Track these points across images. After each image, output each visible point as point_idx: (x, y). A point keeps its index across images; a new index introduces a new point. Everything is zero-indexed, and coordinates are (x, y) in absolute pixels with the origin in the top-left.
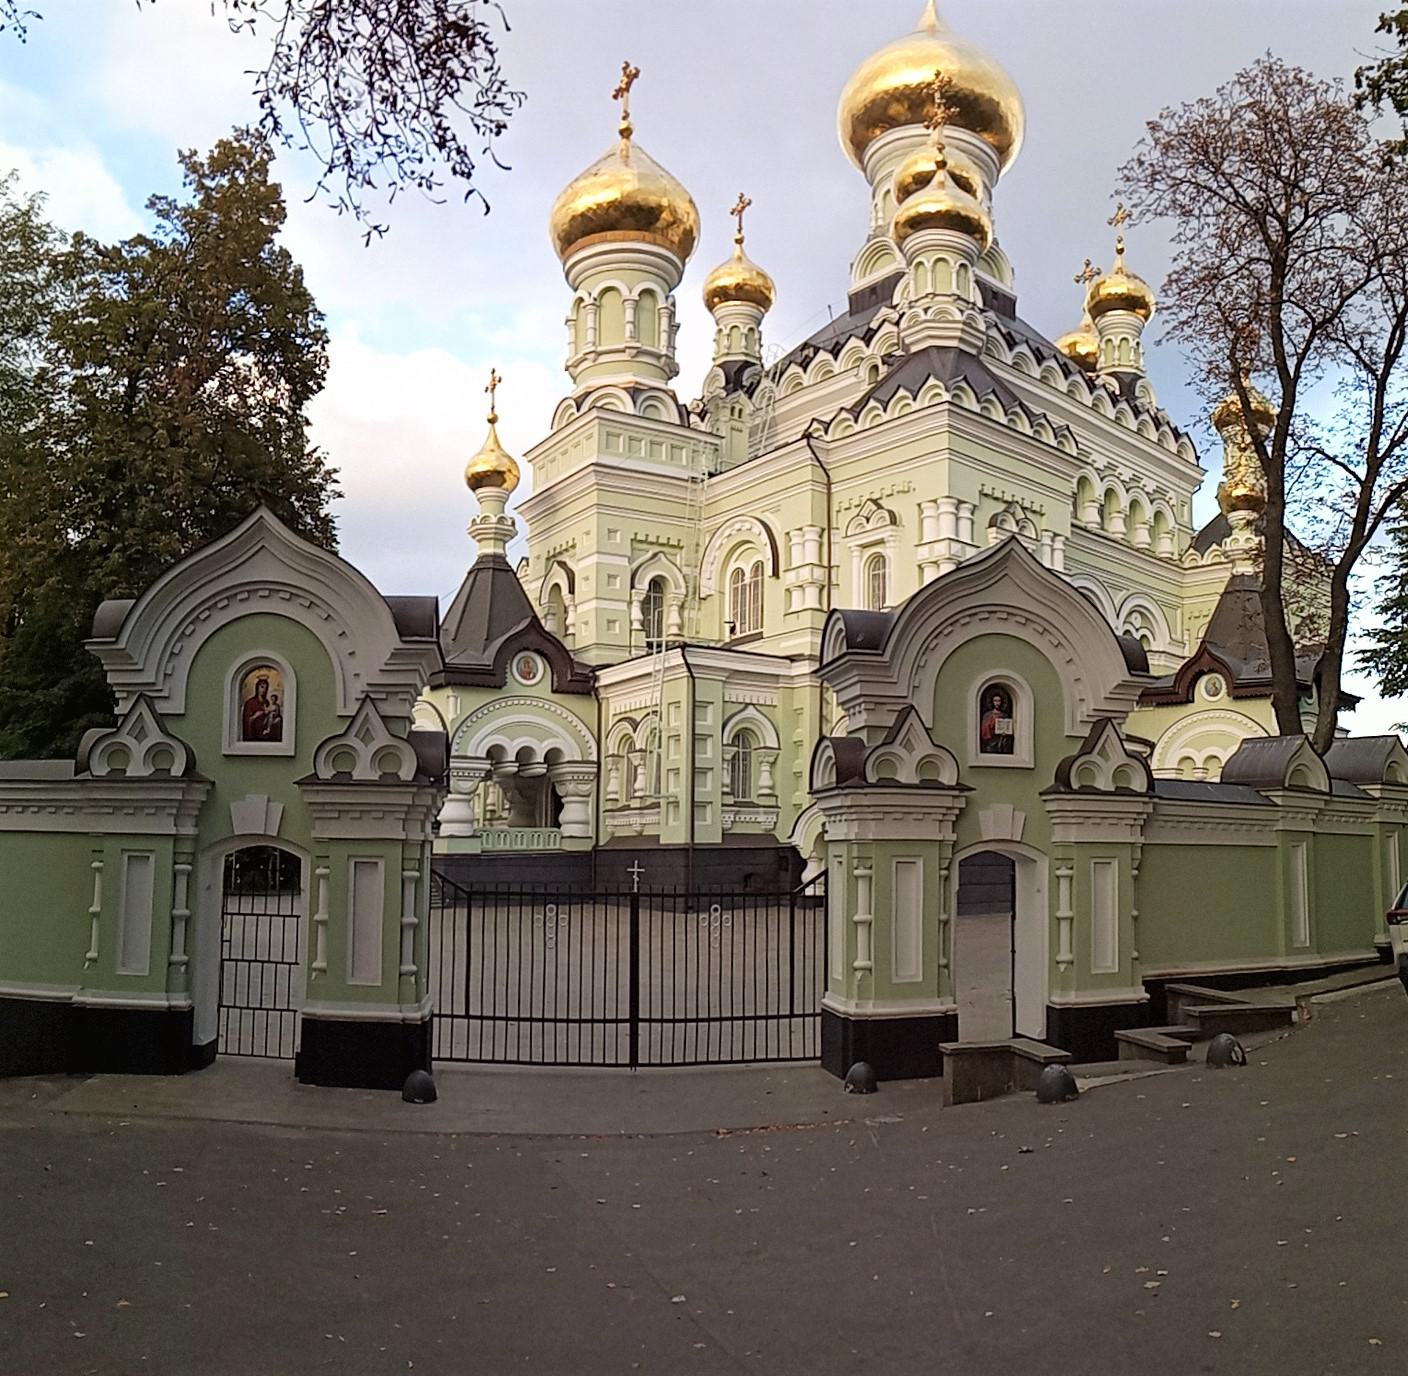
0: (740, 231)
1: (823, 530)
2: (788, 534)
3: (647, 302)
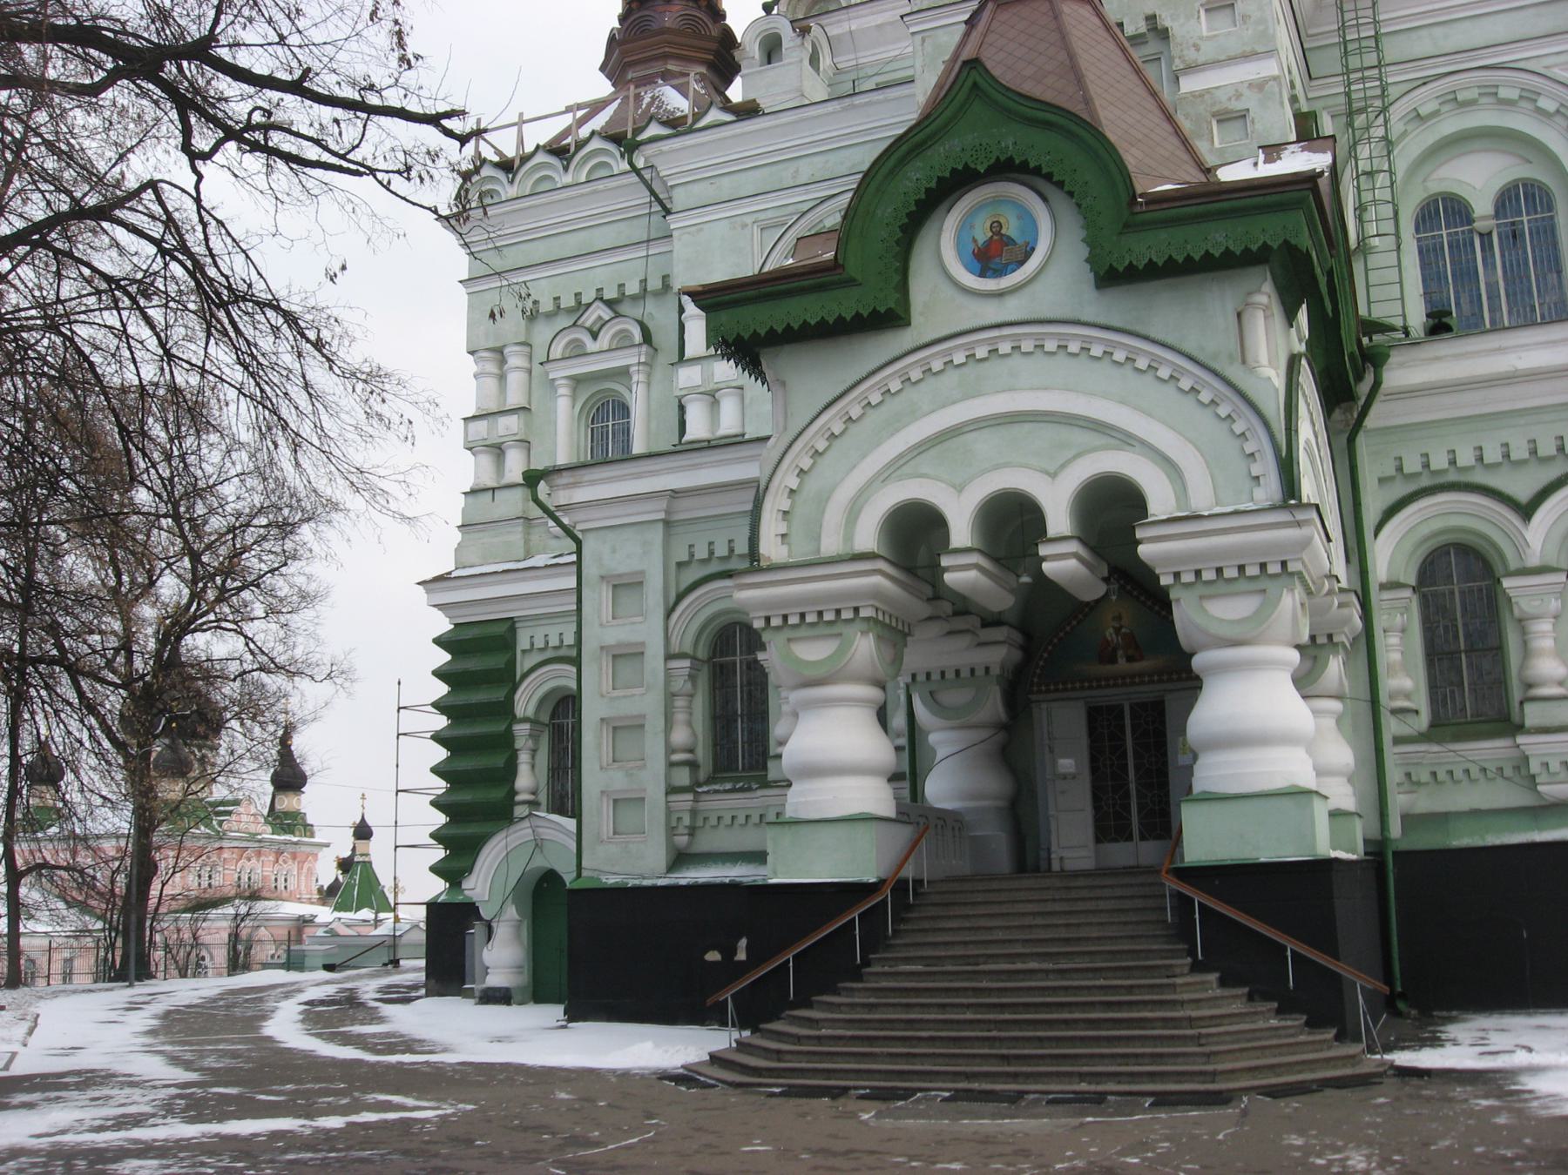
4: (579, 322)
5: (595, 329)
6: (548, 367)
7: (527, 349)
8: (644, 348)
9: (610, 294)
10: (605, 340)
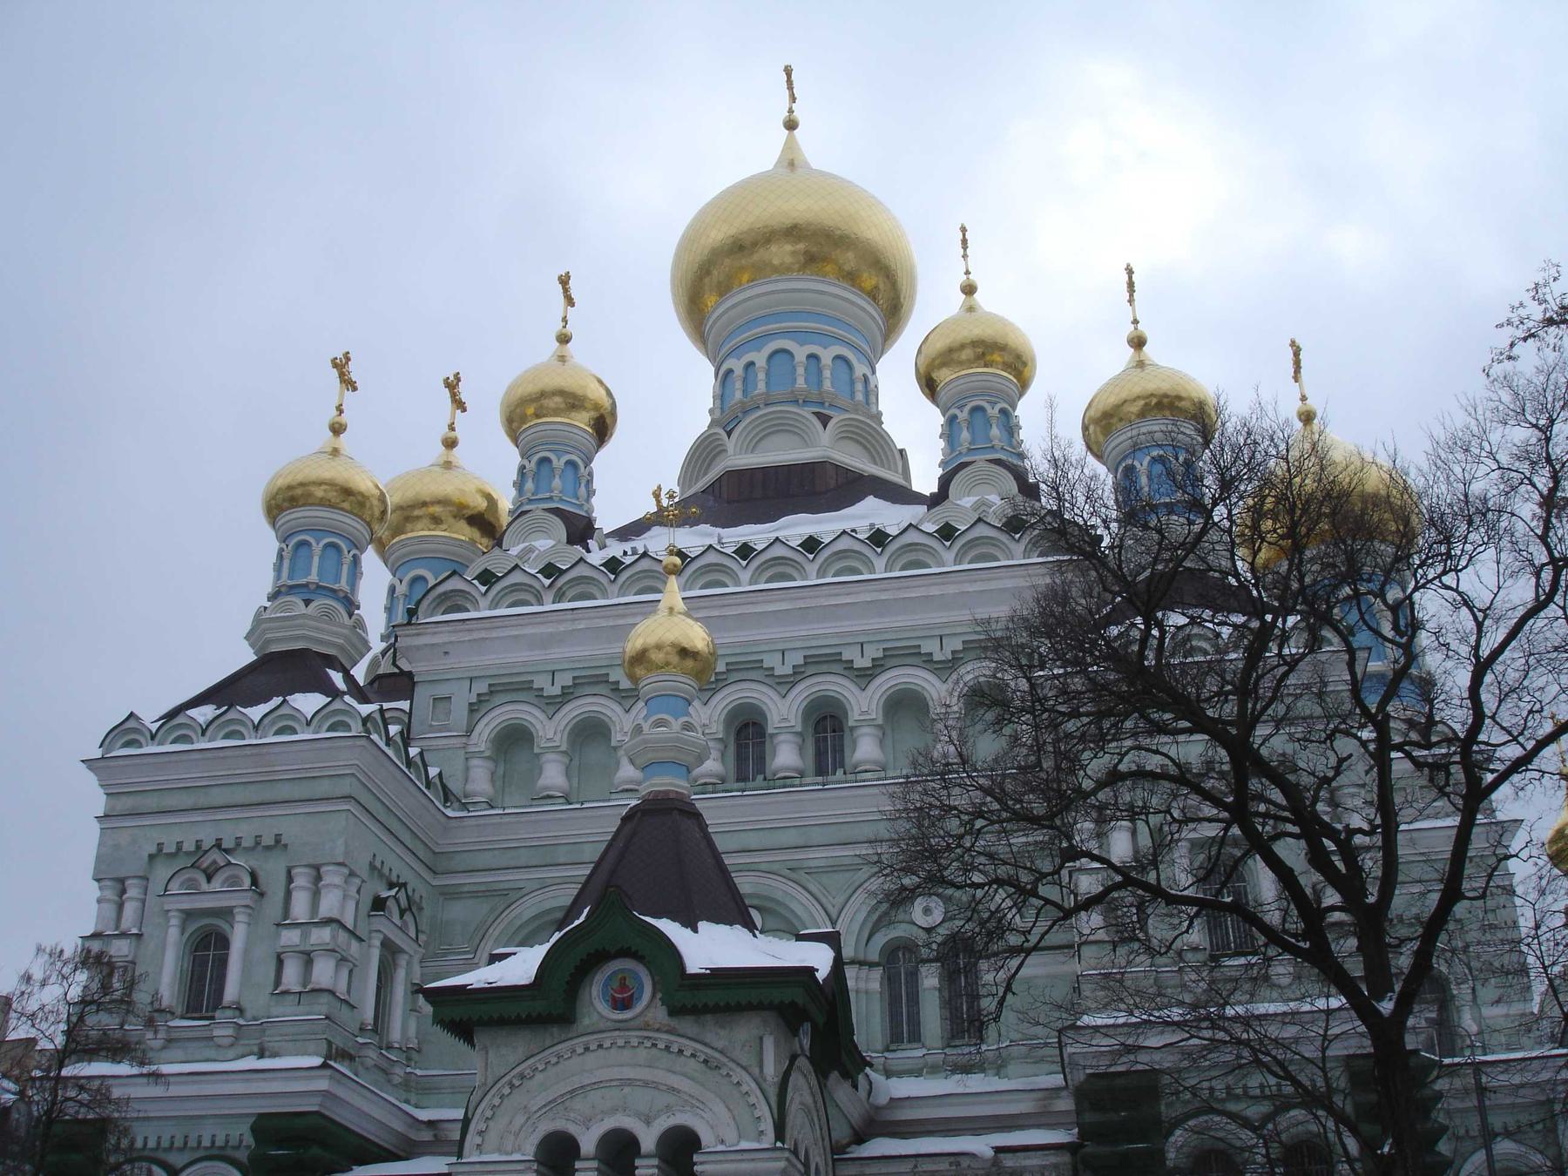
4: (197, 864)
7: (145, 883)
10: (216, 885)
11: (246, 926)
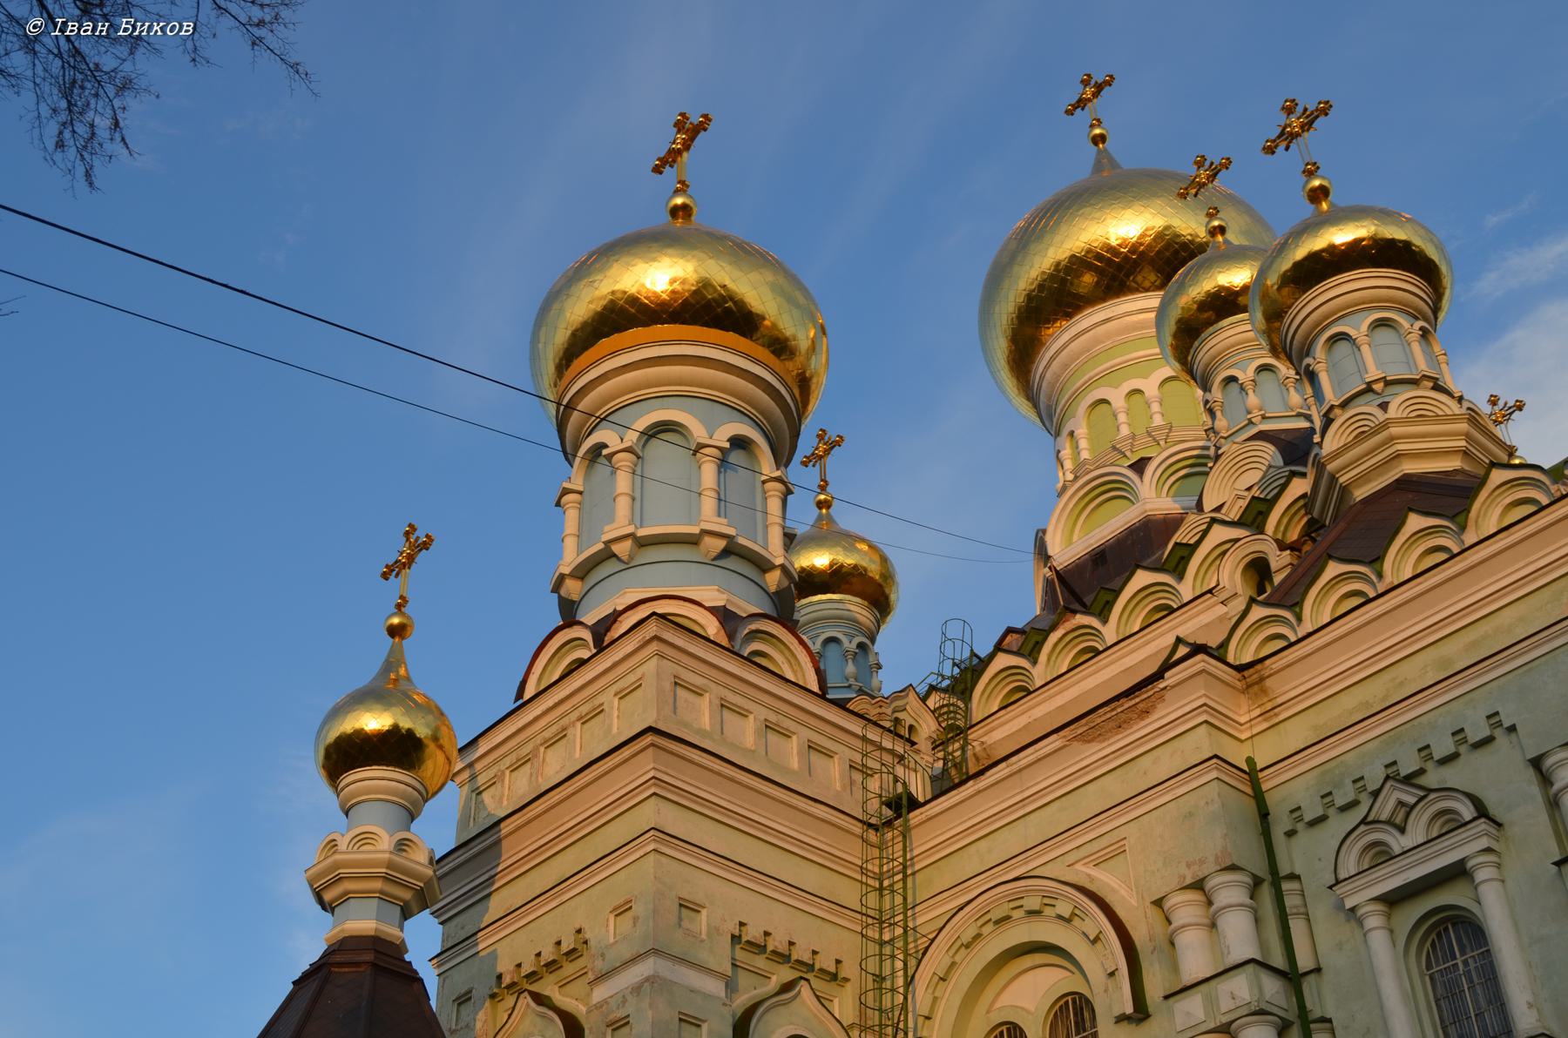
0: (823, 489)
1: (1257, 882)
2: (1158, 903)
3: (736, 457)
4: (1370, 818)
5: (1398, 820)
6: (1339, 890)
8: (1482, 825)
9: (1407, 767)
10: (1417, 831)
11: (1497, 885)
